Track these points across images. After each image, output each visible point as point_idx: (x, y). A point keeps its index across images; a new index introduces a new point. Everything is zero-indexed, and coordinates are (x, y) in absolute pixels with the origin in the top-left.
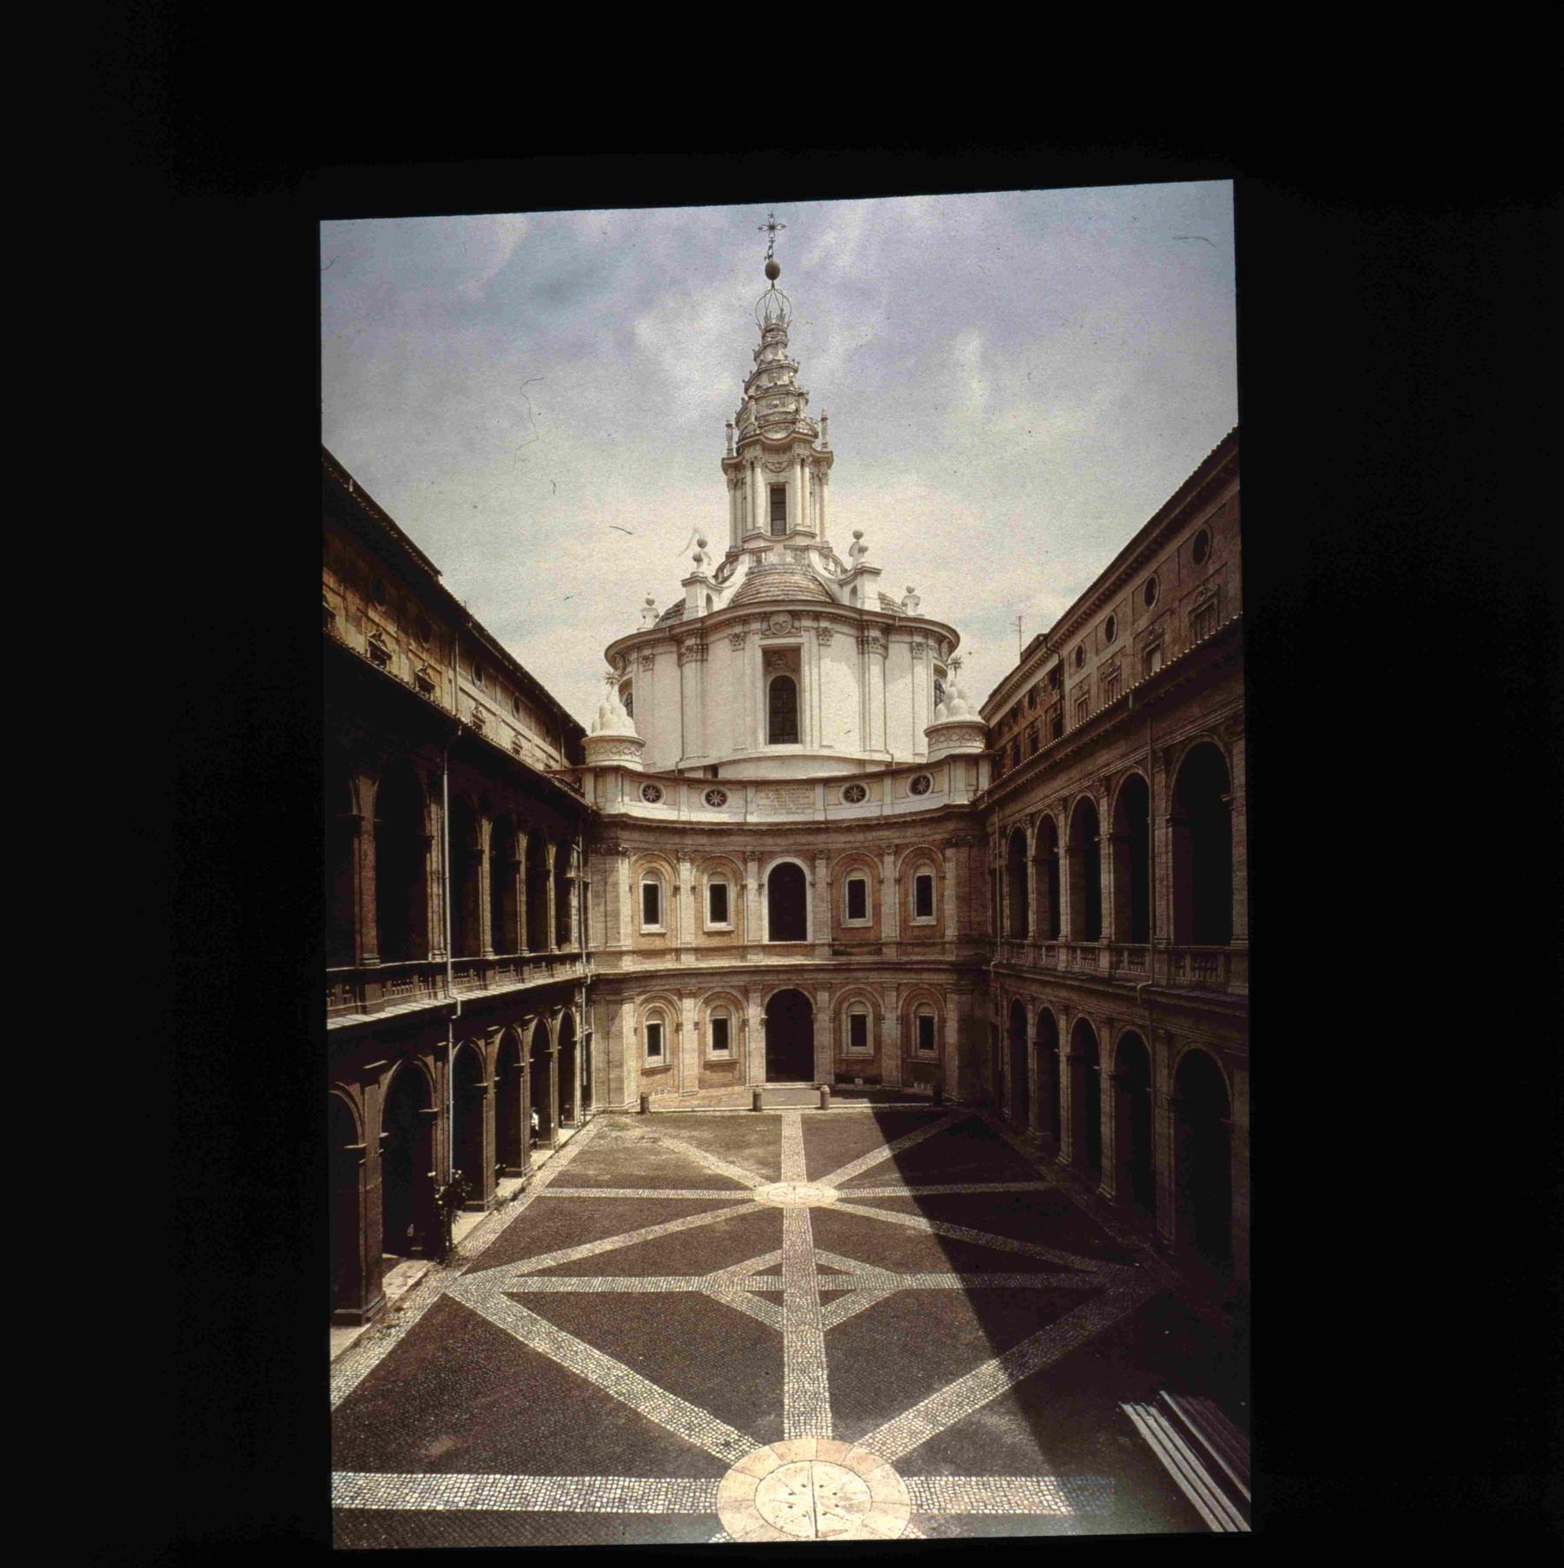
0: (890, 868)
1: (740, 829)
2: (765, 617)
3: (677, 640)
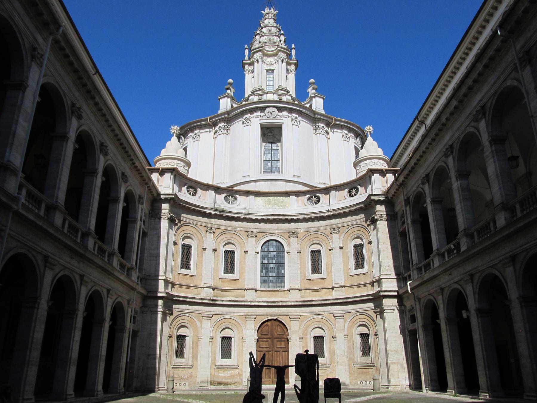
0: (336, 241)
2: (262, 109)
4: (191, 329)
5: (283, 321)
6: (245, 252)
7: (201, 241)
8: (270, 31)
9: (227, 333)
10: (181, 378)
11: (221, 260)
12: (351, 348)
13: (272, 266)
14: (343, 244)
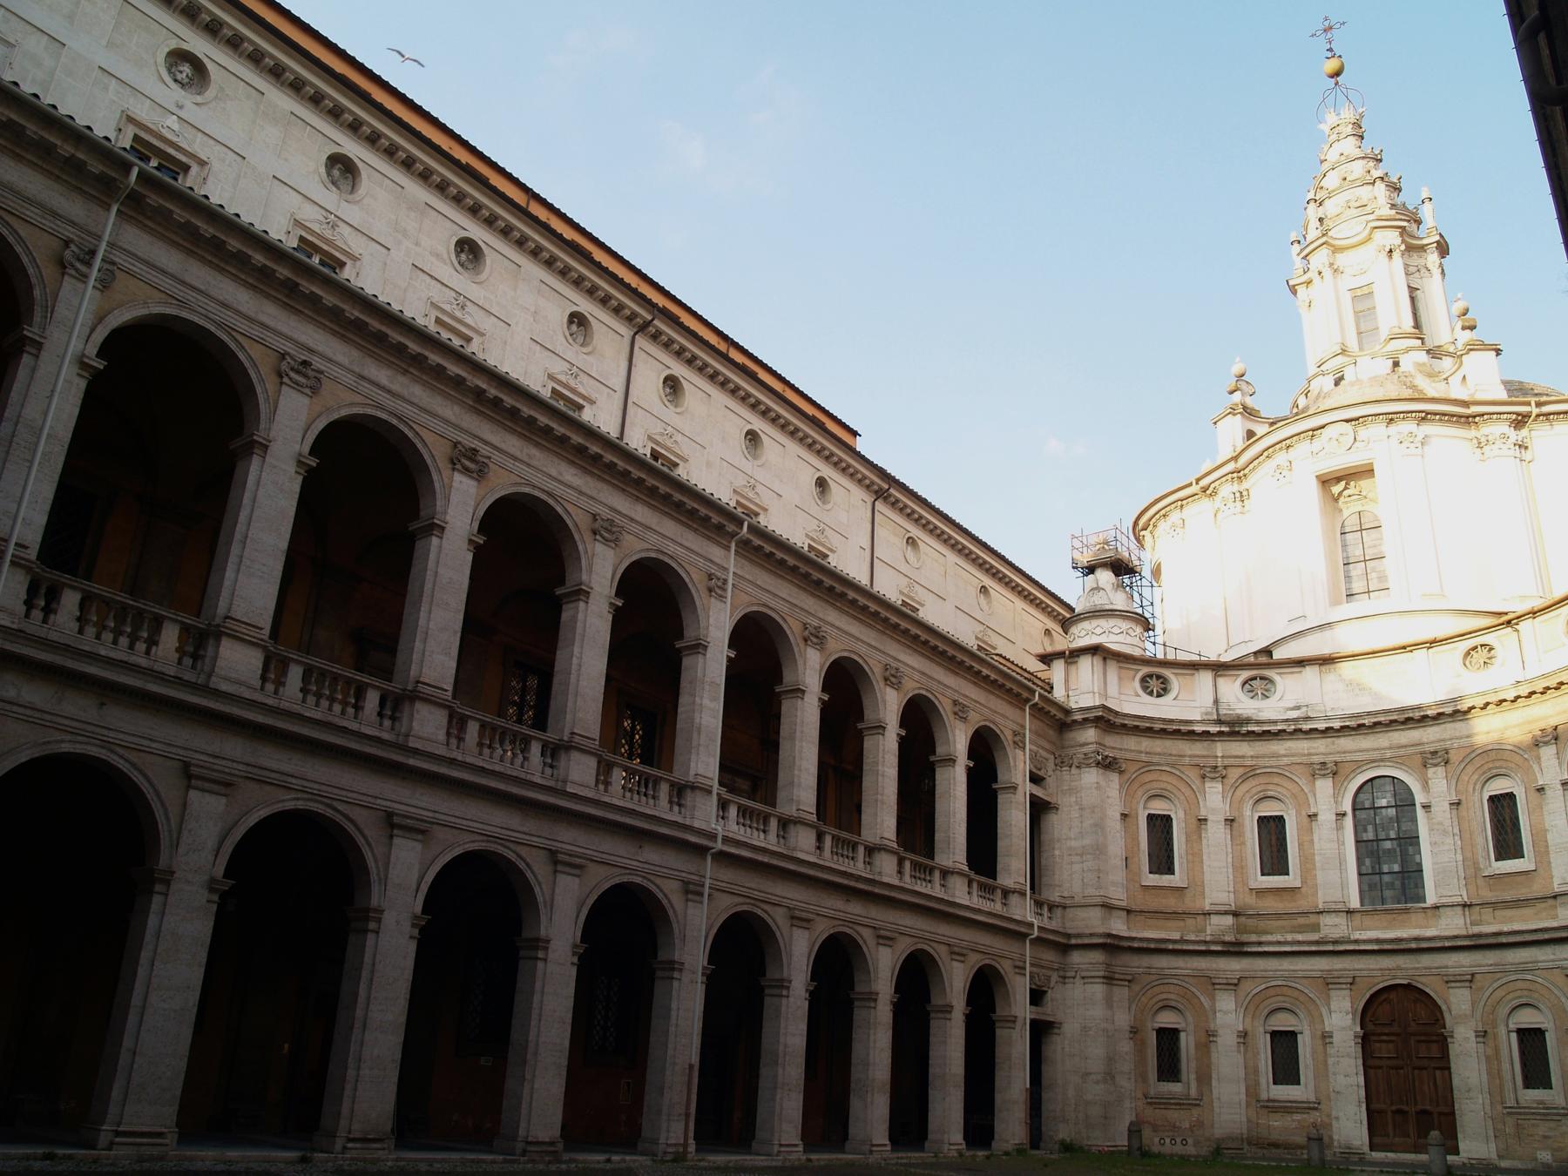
4: (1188, 1015)
7: (1193, 802)
9: (1283, 1022)
11: (1249, 844)
13: (1388, 845)
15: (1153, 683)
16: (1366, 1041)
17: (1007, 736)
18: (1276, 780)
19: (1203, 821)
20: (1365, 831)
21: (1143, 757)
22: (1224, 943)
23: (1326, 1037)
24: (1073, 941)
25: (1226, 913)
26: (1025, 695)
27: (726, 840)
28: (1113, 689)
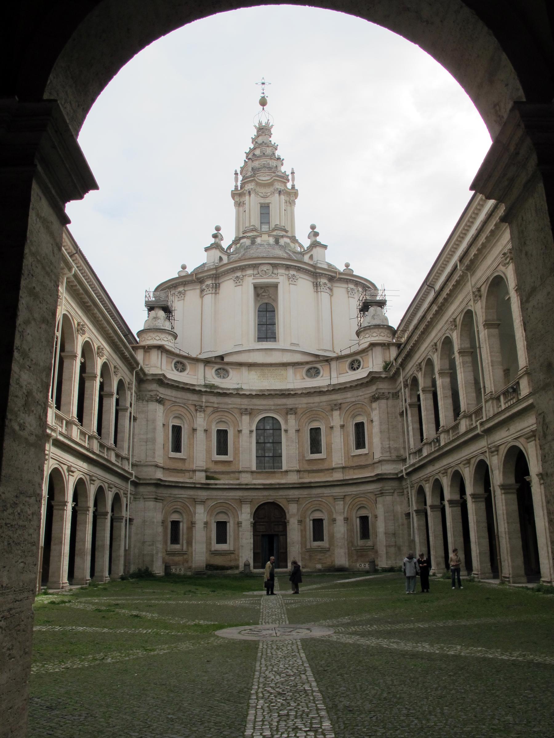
0: (336, 419)
1: (238, 394)
3: (201, 281)
4: (184, 515)
5: (280, 504)
6: (238, 431)
8: (264, 154)
9: (222, 518)
10: (176, 564)
12: (350, 531)
14: (343, 422)
15: (180, 366)
16: (255, 525)
17: (126, 385)
18: (226, 414)
19: (194, 430)
20: (260, 439)
21: (173, 399)
22: (202, 484)
23: (239, 524)
24: (141, 482)
25: (202, 471)
26: (135, 366)
27: (61, 434)
28: (164, 367)
